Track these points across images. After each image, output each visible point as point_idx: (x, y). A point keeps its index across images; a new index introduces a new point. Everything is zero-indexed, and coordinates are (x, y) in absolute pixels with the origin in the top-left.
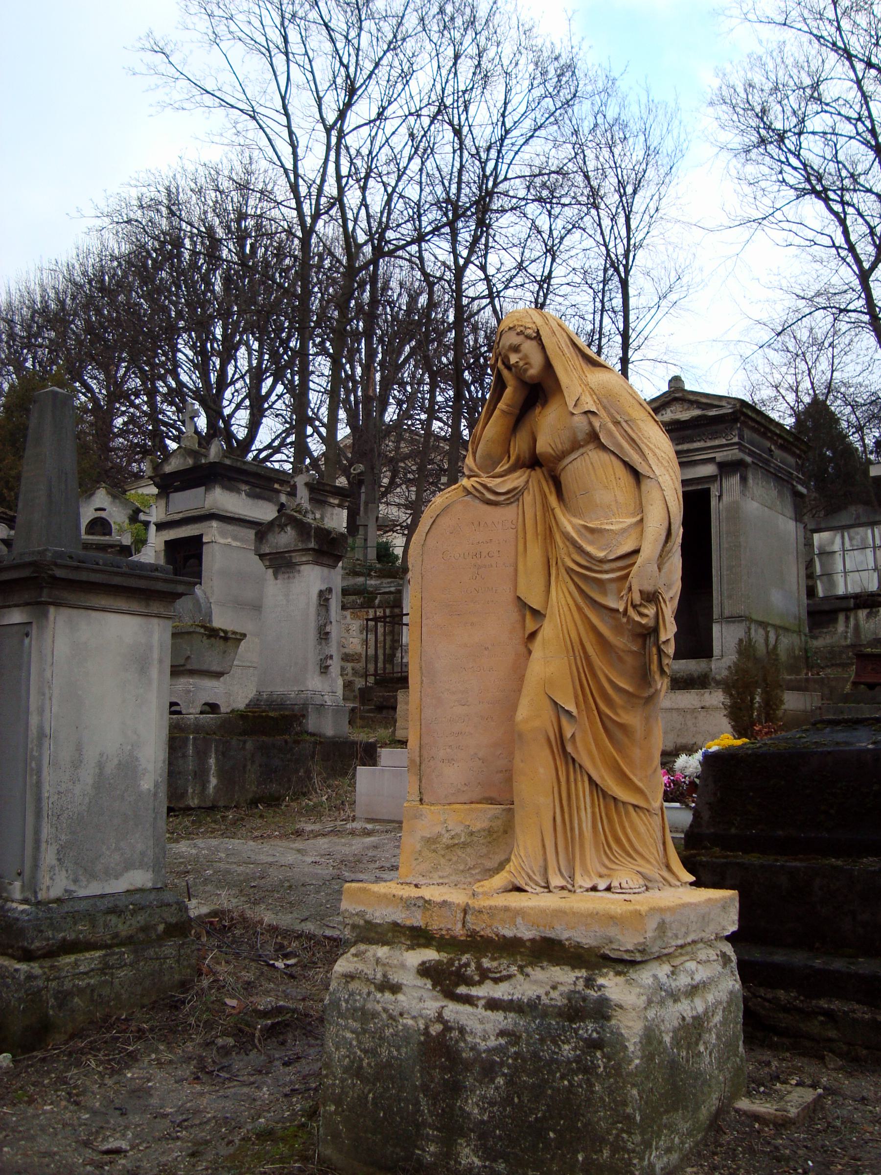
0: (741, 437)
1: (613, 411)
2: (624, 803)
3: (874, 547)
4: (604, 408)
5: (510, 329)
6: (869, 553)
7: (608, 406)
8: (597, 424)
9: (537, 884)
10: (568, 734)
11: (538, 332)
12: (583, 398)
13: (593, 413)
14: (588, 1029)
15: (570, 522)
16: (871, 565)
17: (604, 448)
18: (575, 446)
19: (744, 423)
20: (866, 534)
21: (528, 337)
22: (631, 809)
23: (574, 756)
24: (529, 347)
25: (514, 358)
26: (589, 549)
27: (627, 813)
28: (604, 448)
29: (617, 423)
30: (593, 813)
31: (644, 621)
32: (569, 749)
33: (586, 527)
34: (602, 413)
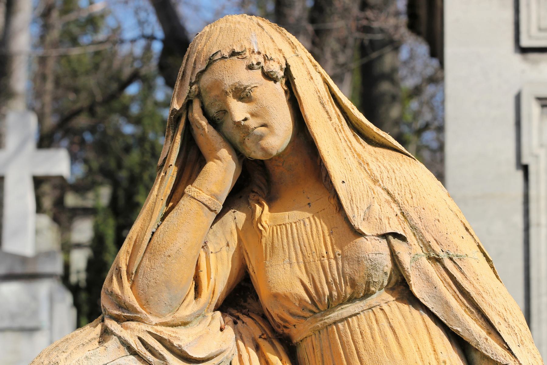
1: (429, 237)
4: (413, 228)
5: (234, 54)
7: (420, 226)
11: (287, 71)
12: (376, 207)
13: (396, 235)
17: (414, 301)
18: (360, 292)
21: (268, 76)
24: (274, 96)
25: (239, 111)
28: (414, 301)
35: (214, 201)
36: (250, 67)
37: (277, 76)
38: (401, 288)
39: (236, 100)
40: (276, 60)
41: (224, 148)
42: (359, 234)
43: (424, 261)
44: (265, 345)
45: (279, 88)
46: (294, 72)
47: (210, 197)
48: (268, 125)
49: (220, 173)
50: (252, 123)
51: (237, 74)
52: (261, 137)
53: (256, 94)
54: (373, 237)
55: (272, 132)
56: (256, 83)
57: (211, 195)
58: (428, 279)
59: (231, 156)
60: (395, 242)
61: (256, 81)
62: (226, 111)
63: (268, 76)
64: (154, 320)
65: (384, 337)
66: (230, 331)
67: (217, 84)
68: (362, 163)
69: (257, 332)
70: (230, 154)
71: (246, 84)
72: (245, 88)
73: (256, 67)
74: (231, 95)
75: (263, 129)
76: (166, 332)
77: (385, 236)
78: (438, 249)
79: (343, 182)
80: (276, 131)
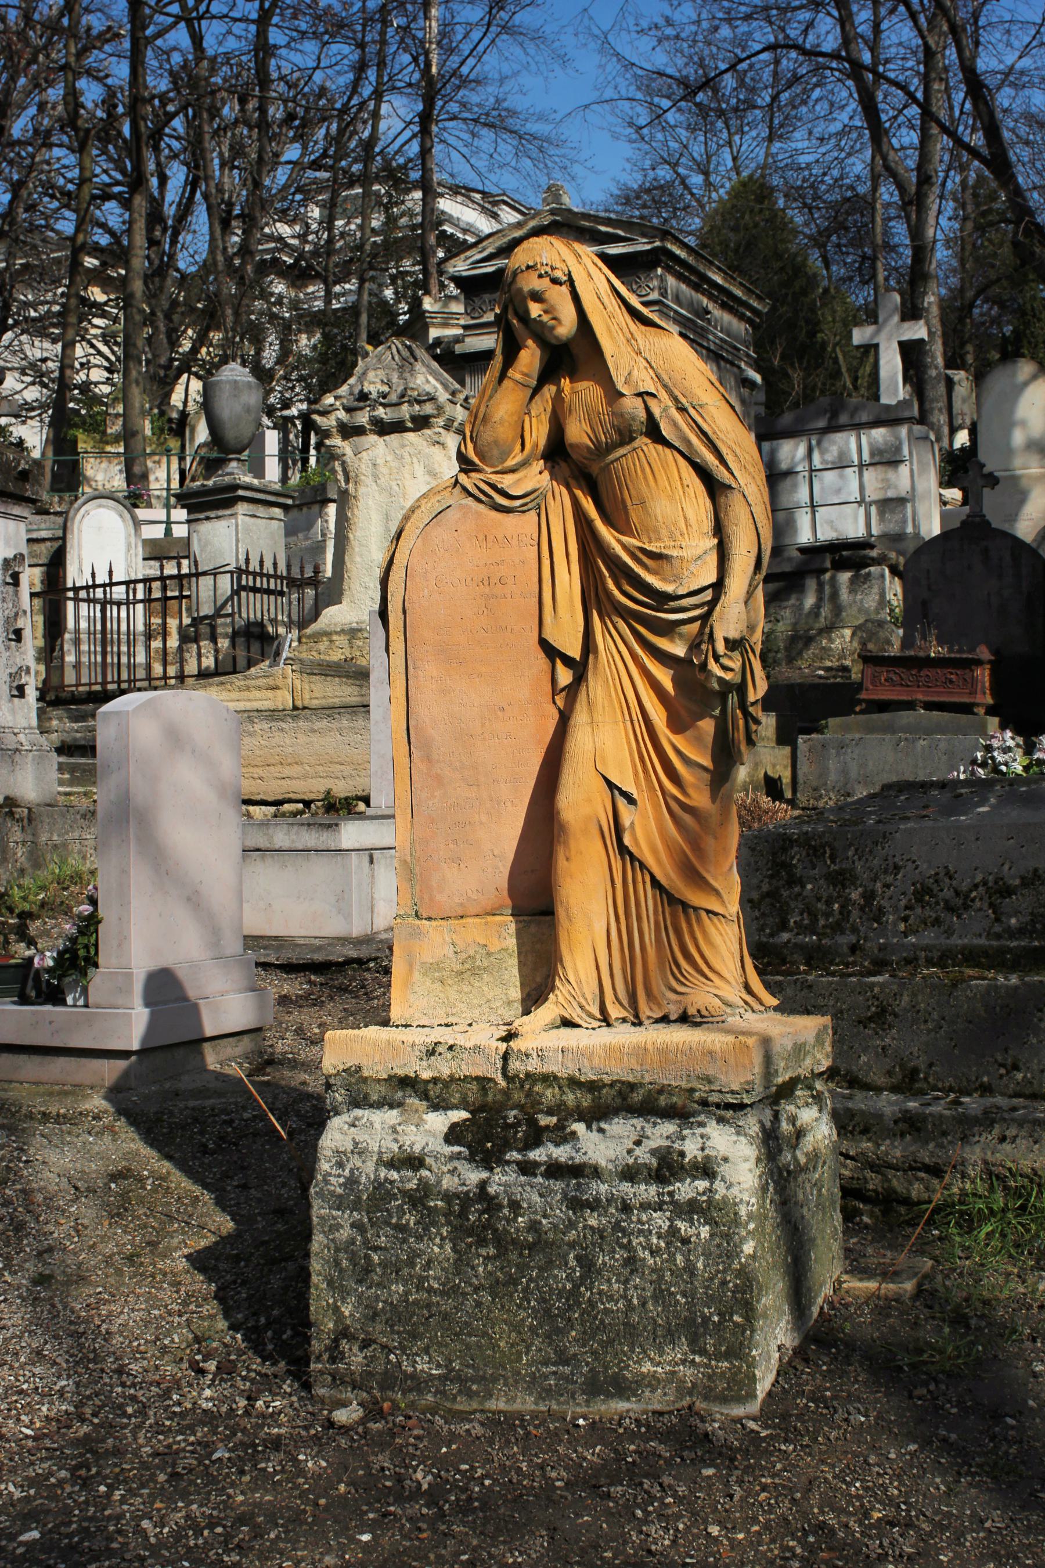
0: (664, 293)
1: (677, 393)
2: (696, 909)
3: (861, 466)
4: (665, 387)
5: (528, 267)
6: (851, 473)
8: (657, 411)
9: (590, 1015)
10: (626, 820)
11: (570, 274)
12: (635, 372)
14: (686, 1190)
15: (619, 541)
16: (856, 495)
18: (625, 436)
19: (668, 269)
20: (847, 443)
21: (555, 281)
22: (703, 914)
23: (633, 849)
24: (560, 297)
25: (535, 310)
26: (650, 579)
27: (699, 920)
29: (682, 410)
30: (657, 923)
31: (728, 676)
32: (627, 840)
33: (643, 550)
34: (663, 395)
36: (540, 276)
38: (653, 432)
42: (622, 395)
43: (673, 412)
44: (572, 482)
45: (565, 289)
46: (574, 276)
49: (530, 358)
50: (545, 318)
51: (531, 282)
52: (553, 328)
53: (547, 295)
58: (675, 425)
62: (527, 311)
63: (555, 281)
64: (489, 470)
65: (643, 470)
66: (546, 475)
67: (520, 290)
68: (631, 339)
69: (567, 473)
76: (494, 478)
77: (640, 395)
78: (684, 401)
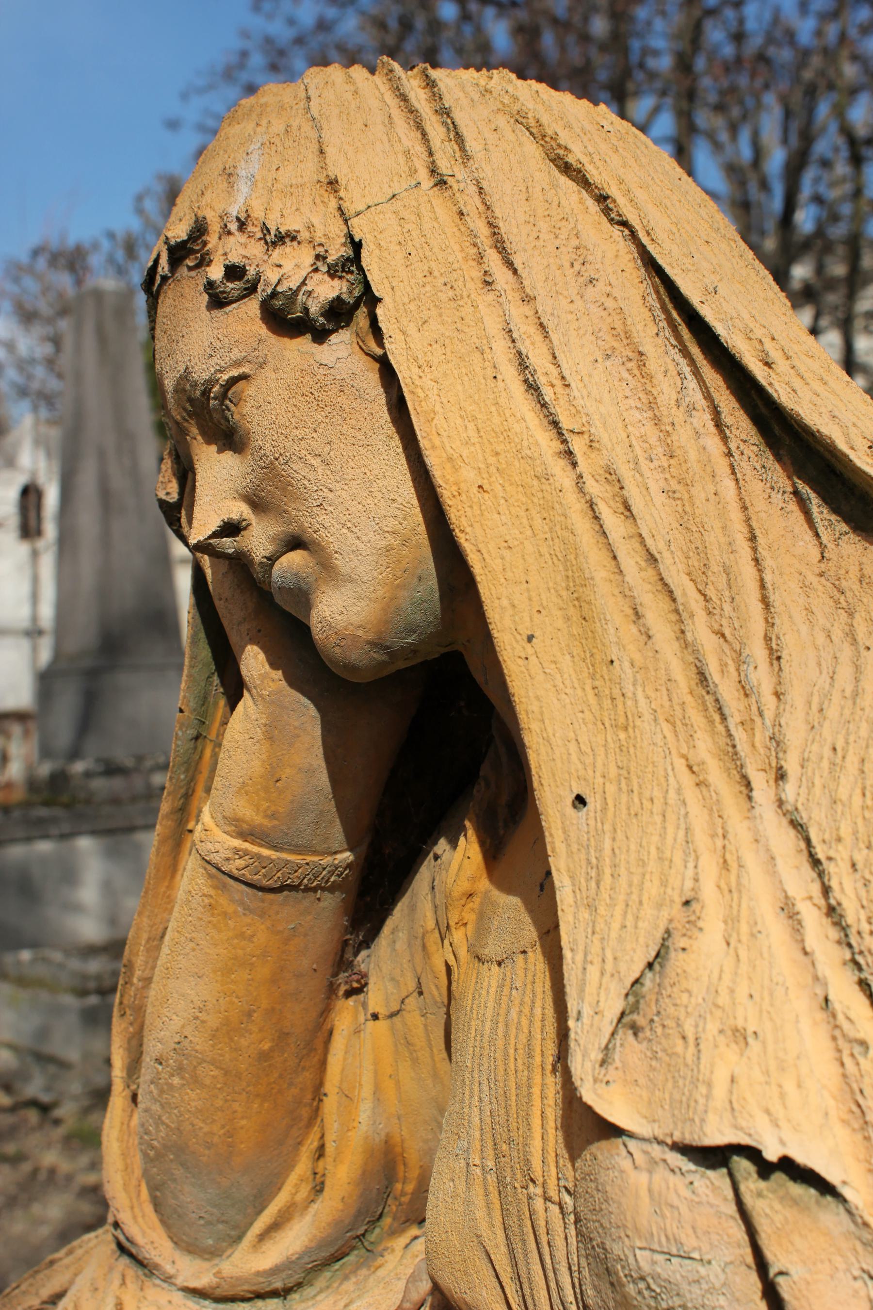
35: (259, 856)
37: (306, 310)
39: (214, 448)
40: (304, 235)
41: (252, 641)
47: (237, 843)
48: (306, 537)
54: (656, 1151)
55: (326, 565)
56: (237, 363)
57: (243, 835)
59: (278, 674)
60: (769, 1200)
61: (236, 354)
70: (274, 665)
71: (205, 376)
72: (206, 393)
73: (233, 287)
74: (194, 430)
75: (295, 559)
77: (713, 1157)
79: (580, 800)
80: (339, 561)
